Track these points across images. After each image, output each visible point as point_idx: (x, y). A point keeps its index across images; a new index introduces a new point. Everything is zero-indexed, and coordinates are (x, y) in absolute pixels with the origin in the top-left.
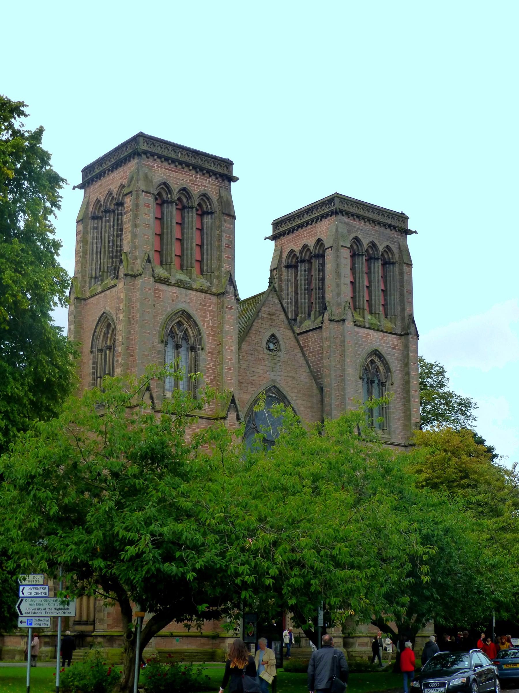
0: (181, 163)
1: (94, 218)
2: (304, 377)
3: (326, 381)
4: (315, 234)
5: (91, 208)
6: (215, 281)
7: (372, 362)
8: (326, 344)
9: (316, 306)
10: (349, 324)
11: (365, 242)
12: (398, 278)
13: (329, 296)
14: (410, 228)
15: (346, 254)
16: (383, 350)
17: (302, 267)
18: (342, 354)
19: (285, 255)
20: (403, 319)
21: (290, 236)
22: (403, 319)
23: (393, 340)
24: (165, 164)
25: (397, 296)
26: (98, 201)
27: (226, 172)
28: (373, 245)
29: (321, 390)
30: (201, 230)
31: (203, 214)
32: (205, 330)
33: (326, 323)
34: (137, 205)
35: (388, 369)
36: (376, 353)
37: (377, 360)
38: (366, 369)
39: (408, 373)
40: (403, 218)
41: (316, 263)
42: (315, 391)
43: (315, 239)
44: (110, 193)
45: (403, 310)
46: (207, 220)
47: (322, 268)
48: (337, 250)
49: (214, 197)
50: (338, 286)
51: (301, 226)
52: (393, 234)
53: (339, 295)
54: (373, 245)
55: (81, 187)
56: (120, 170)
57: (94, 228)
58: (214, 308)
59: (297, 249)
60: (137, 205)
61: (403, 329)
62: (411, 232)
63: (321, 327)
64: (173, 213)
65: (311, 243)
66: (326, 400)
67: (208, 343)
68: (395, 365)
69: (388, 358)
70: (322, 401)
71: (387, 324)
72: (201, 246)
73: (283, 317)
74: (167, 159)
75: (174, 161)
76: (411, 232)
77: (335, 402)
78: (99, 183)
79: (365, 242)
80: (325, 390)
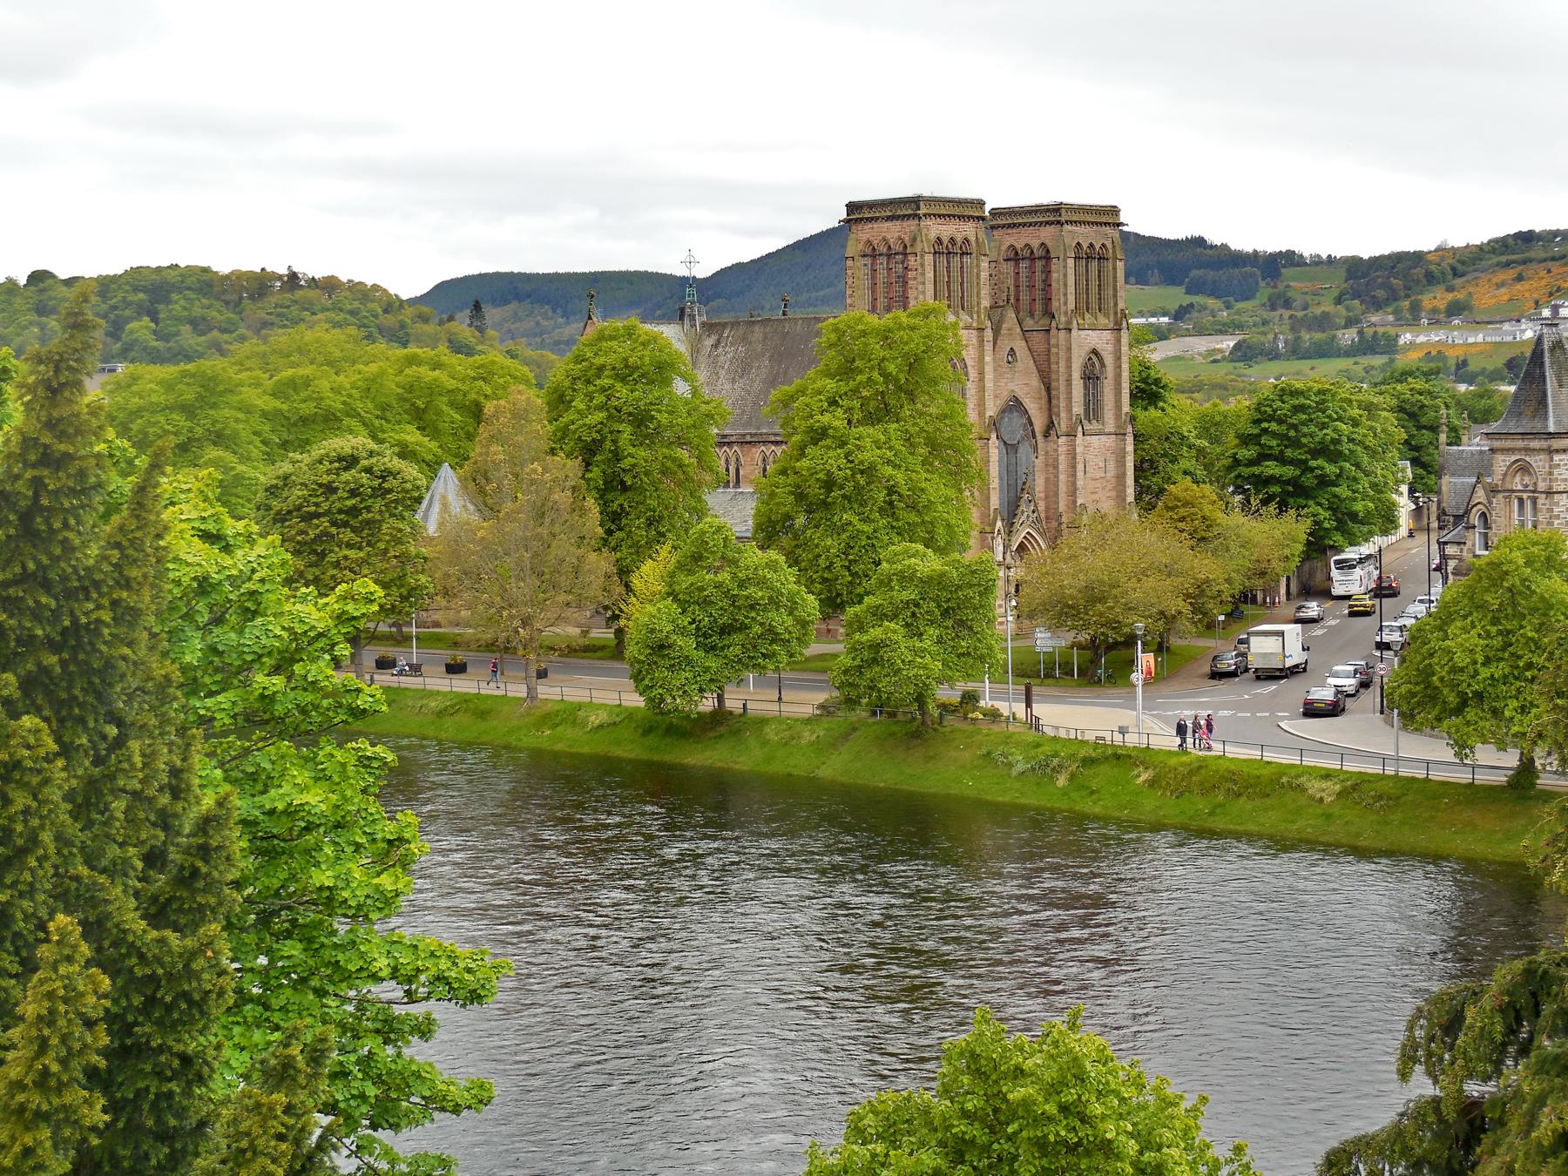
0: (949, 216)
2: (1035, 382)
3: (1054, 384)
6: (975, 317)
7: (1090, 359)
8: (1054, 350)
9: (1038, 306)
10: (1075, 332)
11: (1085, 246)
12: (1111, 274)
13: (1055, 304)
14: (1122, 220)
15: (1071, 262)
16: (1099, 348)
17: (1023, 264)
18: (1069, 360)
19: (1004, 248)
20: (1116, 313)
21: (1010, 231)
22: (1116, 313)
23: (1107, 335)
25: (1111, 293)
27: (981, 214)
28: (1091, 245)
29: (1048, 390)
30: (962, 267)
31: (962, 254)
32: (969, 363)
33: (1053, 332)
35: (1103, 365)
36: (1095, 352)
37: (1094, 357)
38: (1086, 366)
39: (1120, 367)
40: (1114, 211)
41: (1039, 264)
42: (1044, 393)
43: (1040, 242)
44: (884, 239)
45: (1116, 305)
46: (966, 259)
47: (1047, 272)
48: (1065, 260)
49: (973, 239)
50: (1065, 295)
51: (1024, 225)
52: (1108, 230)
53: (1066, 303)
54: (1091, 245)
56: (895, 222)
58: (975, 341)
59: (1019, 246)
60: (922, 265)
61: (1116, 323)
63: (1048, 331)
64: (944, 259)
65: (1035, 244)
66: (1054, 402)
67: (973, 374)
68: (1109, 360)
69: (1102, 353)
70: (1050, 401)
71: (1103, 321)
72: (962, 284)
73: (1018, 330)
75: (944, 216)
77: (1063, 404)
79: (1085, 246)
80: (1053, 393)
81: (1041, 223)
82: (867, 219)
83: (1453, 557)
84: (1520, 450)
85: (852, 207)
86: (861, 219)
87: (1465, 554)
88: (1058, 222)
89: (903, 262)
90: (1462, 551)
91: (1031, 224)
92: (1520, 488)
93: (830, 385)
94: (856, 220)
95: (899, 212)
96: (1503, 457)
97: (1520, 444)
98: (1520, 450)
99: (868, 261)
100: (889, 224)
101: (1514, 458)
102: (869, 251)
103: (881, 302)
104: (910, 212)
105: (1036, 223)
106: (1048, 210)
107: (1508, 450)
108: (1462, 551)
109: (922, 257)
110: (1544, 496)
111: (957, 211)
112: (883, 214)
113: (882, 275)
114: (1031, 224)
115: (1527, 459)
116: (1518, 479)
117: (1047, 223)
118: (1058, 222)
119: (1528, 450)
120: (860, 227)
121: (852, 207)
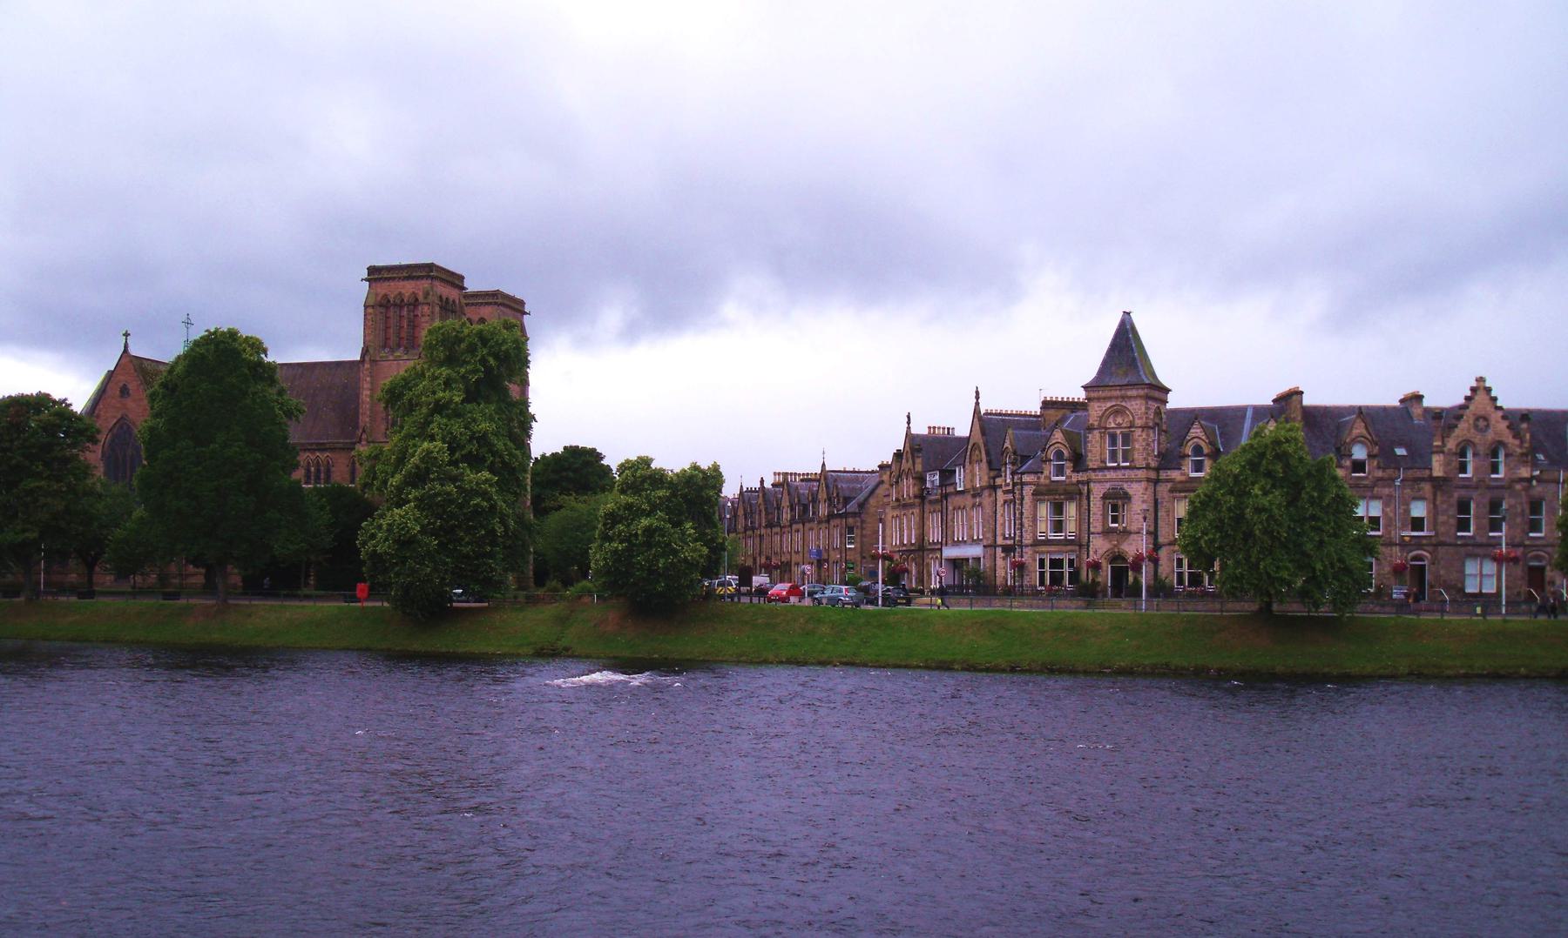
1: (380, 306)
4: (479, 314)
5: (379, 298)
24: (443, 284)
26: (385, 296)
34: (433, 313)
40: (522, 303)
43: (479, 317)
44: (400, 293)
49: (457, 302)
55: (366, 280)
56: (411, 282)
57: (381, 313)
60: (433, 313)
62: (525, 313)
74: (442, 280)
76: (525, 313)
78: (387, 283)
81: (482, 303)
82: (386, 279)
83: (1030, 483)
84: (1117, 398)
85: (372, 270)
86: (381, 279)
87: (1042, 480)
88: (496, 303)
89: (413, 311)
90: (1039, 478)
91: (473, 304)
92: (1113, 425)
93: (445, 371)
94: (376, 280)
95: (414, 274)
96: (1099, 404)
97: (1118, 393)
98: (1117, 398)
99: (382, 310)
100: (406, 283)
101: (1109, 405)
102: (384, 302)
103: (393, 339)
104: (424, 274)
105: (477, 304)
106: (481, 295)
107: (1104, 398)
108: (1039, 478)
109: (433, 307)
110: (1140, 429)
111: (450, 279)
112: (400, 275)
113: (393, 322)
114: (473, 304)
115: (1123, 404)
116: (1111, 420)
117: (486, 303)
118: (496, 303)
119: (1123, 398)
120: (379, 284)
121: (372, 270)
